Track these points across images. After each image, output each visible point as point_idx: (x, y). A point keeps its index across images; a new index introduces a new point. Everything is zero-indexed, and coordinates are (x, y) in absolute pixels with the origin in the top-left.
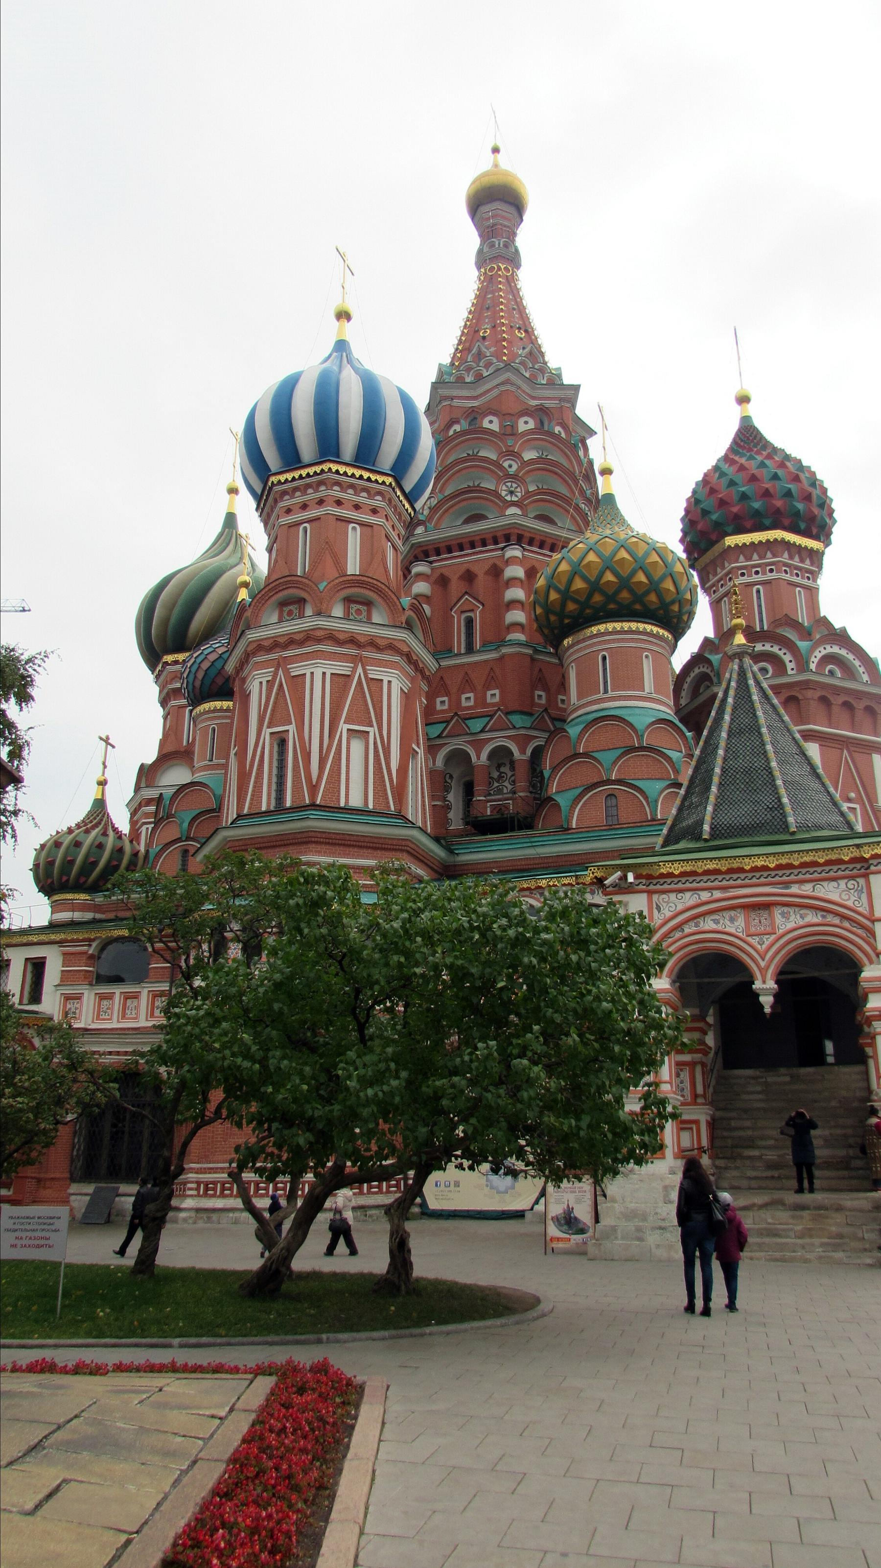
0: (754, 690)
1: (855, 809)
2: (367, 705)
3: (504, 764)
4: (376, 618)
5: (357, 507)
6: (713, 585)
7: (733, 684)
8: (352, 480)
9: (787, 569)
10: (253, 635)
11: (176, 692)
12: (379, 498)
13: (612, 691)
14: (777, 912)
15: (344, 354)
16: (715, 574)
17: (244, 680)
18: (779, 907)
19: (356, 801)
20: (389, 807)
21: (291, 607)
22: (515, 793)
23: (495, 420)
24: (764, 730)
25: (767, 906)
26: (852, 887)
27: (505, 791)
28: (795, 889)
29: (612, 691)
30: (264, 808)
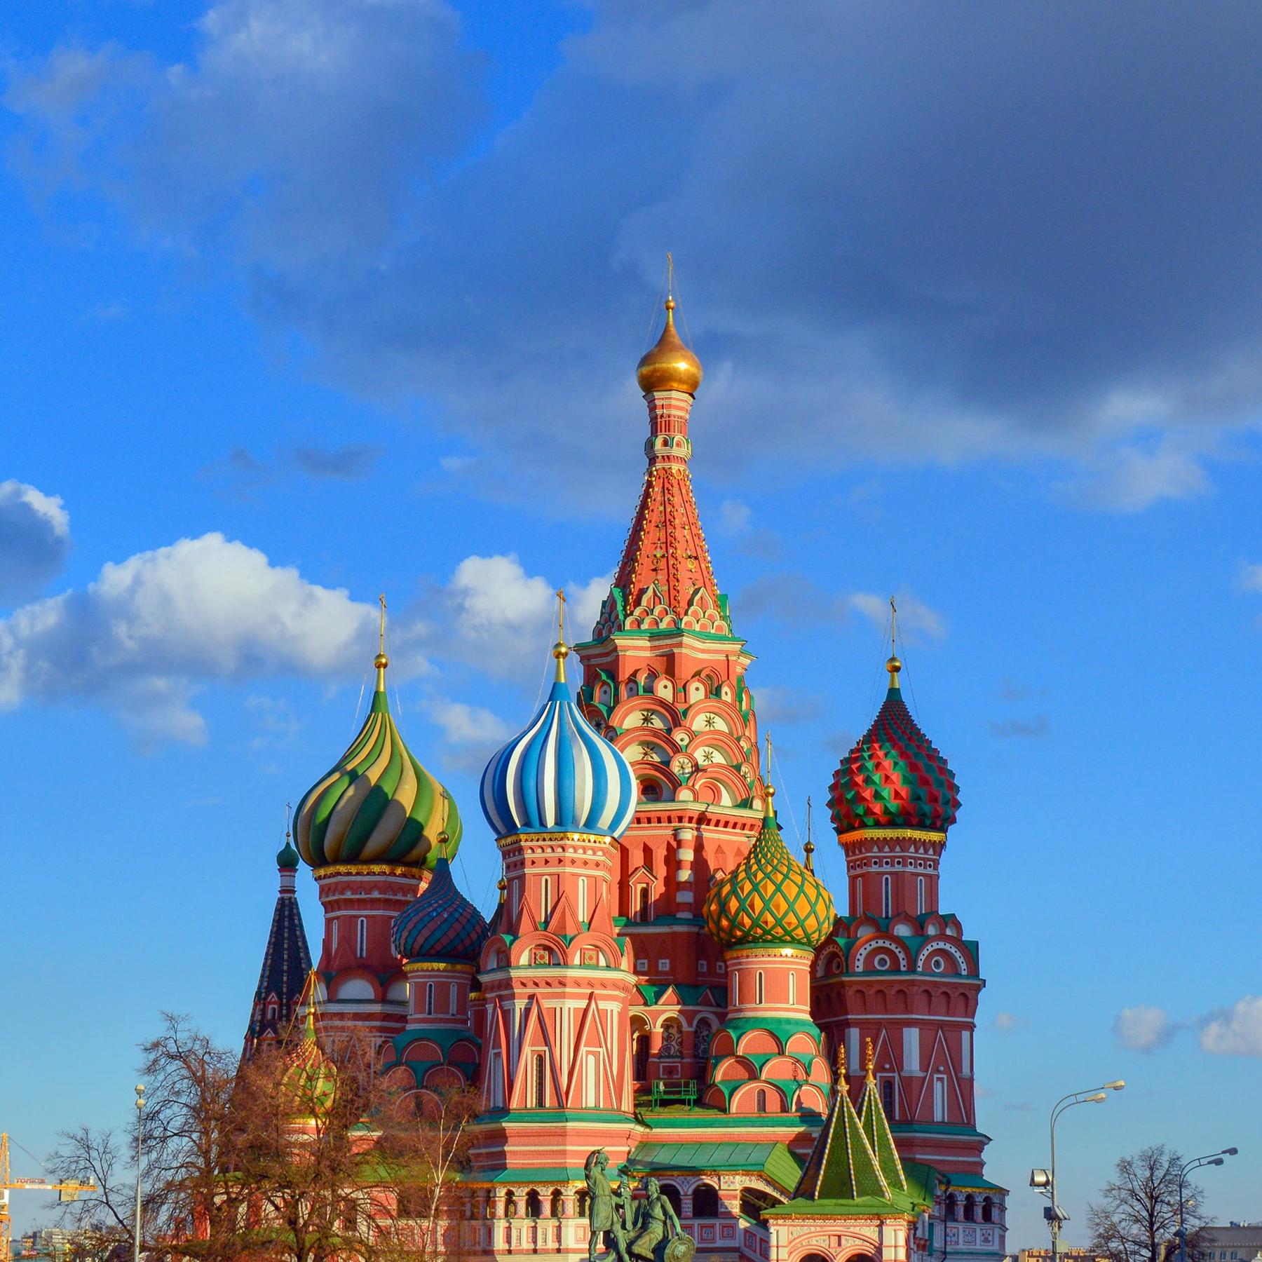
0: (846, 1115)
1: (943, 1078)
2: (598, 1032)
3: (672, 1027)
4: (602, 962)
6: (851, 861)
8: (583, 844)
9: (913, 861)
10: (514, 973)
11: (349, 904)
12: (600, 853)
14: (843, 1238)
16: (854, 854)
19: (591, 1103)
20: (612, 1105)
21: (542, 952)
22: (682, 1059)
27: (672, 1052)
28: (852, 1229)
29: (766, 1002)
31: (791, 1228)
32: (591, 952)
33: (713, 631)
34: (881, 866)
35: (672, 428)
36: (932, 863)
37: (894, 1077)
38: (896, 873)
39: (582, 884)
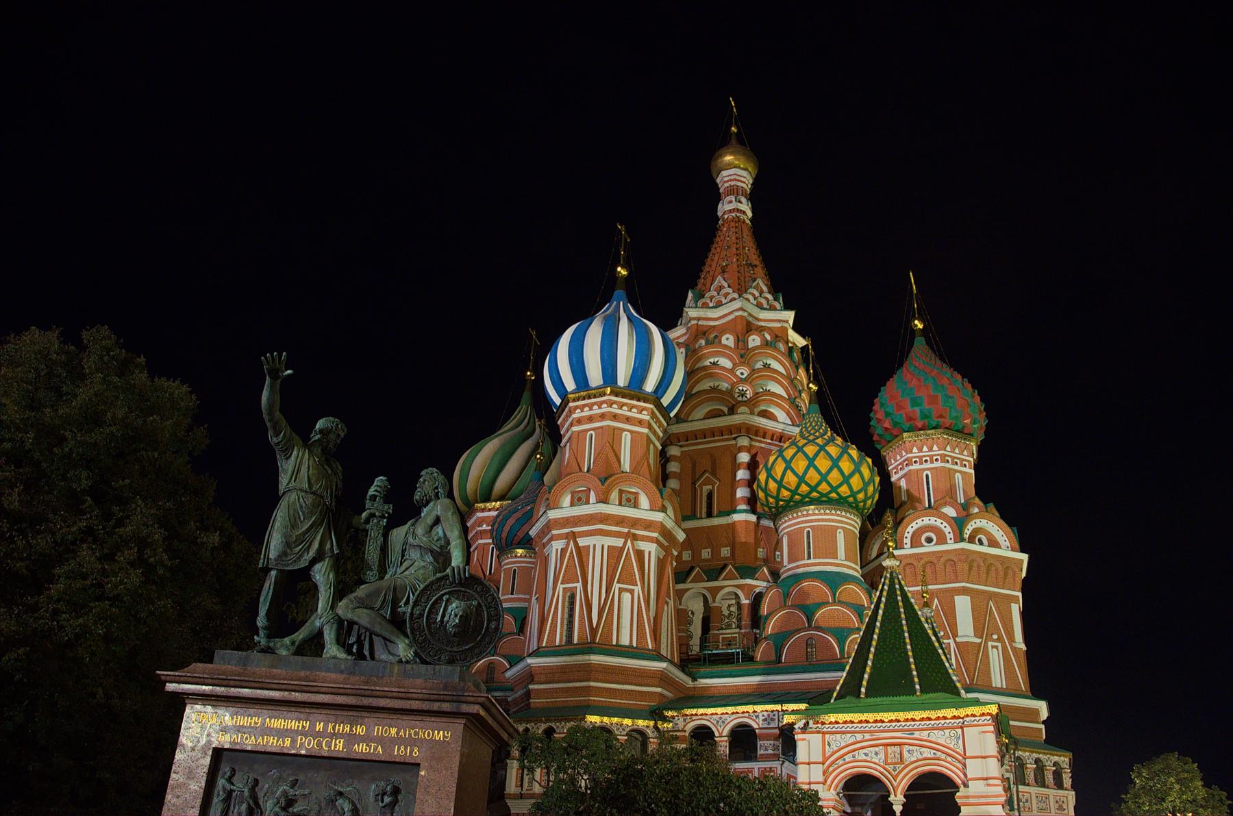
0: (898, 592)
1: (997, 646)
5: (628, 420)
7: (886, 587)
10: (553, 514)
12: (645, 412)
13: (814, 558)
15: (621, 303)
16: (896, 461)
17: (544, 546)
18: (907, 746)
19: (625, 641)
20: (648, 646)
22: (741, 629)
23: (731, 338)
24: (904, 622)
25: (900, 745)
26: (953, 735)
27: (734, 627)
28: (917, 735)
29: (814, 558)
30: (557, 644)
31: (827, 736)
32: (629, 496)
33: (768, 307)
34: (921, 463)
35: (735, 192)
36: (967, 463)
37: (949, 643)
38: (936, 468)
39: (626, 439)
